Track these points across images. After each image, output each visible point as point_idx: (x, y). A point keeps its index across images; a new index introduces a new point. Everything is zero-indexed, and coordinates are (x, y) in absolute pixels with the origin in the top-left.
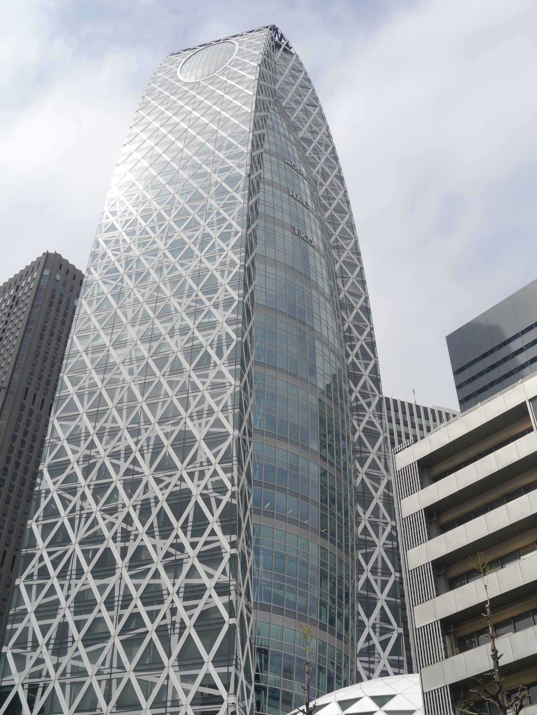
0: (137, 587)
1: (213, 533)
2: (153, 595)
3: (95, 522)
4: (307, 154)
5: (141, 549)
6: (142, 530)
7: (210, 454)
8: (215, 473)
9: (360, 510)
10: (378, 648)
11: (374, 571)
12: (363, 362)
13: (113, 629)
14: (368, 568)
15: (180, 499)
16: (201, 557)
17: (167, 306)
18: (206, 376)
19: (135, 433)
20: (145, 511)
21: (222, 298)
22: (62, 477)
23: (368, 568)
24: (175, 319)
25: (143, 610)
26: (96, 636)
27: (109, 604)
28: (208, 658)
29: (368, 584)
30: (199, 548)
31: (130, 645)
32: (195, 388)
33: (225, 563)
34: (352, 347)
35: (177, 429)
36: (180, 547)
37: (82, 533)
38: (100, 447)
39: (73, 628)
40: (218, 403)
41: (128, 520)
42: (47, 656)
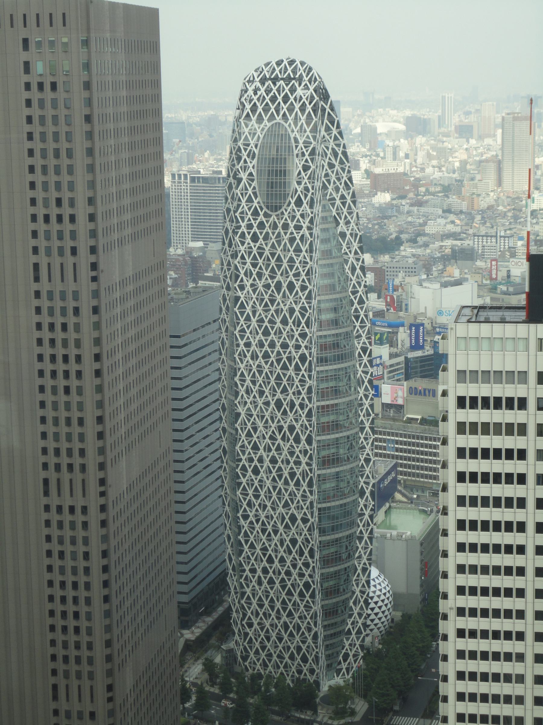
0: (283, 569)
1: (306, 557)
2: (288, 573)
3: (264, 543)
4: (343, 251)
5: (282, 557)
6: (282, 550)
7: (303, 526)
8: (305, 535)
9: (360, 500)
10: (363, 555)
11: (364, 526)
12: (366, 418)
13: (277, 582)
14: (361, 525)
15: (294, 542)
16: (303, 564)
17: (279, 444)
18: (299, 490)
19: (274, 509)
20: (282, 542)
21: (303, 449)
22: (248, 521)
23: (361, 525)
24: (284, 454)
25: (286, 578)
26: (271, 582)
27: (274, 572)
28: (308, 596)
29: (361, 532)
30: (302, 561)
31: (283, 587)
32: (295, 496)
33: (311, 568)
34: (362, 410)
35: (290, 512)
36: (295, 559)
37: (260, 546)
38: (260, 512)
39: (263, 579)
40: (305, 504)
41: (276, 544)
42: (256, 585)
